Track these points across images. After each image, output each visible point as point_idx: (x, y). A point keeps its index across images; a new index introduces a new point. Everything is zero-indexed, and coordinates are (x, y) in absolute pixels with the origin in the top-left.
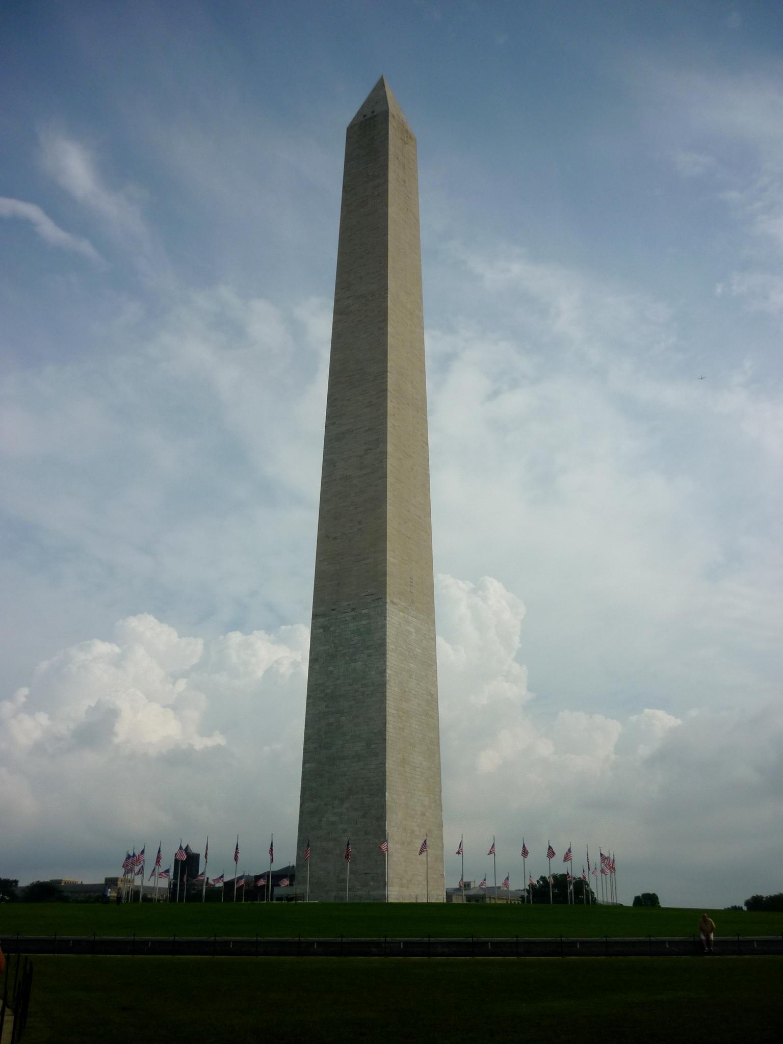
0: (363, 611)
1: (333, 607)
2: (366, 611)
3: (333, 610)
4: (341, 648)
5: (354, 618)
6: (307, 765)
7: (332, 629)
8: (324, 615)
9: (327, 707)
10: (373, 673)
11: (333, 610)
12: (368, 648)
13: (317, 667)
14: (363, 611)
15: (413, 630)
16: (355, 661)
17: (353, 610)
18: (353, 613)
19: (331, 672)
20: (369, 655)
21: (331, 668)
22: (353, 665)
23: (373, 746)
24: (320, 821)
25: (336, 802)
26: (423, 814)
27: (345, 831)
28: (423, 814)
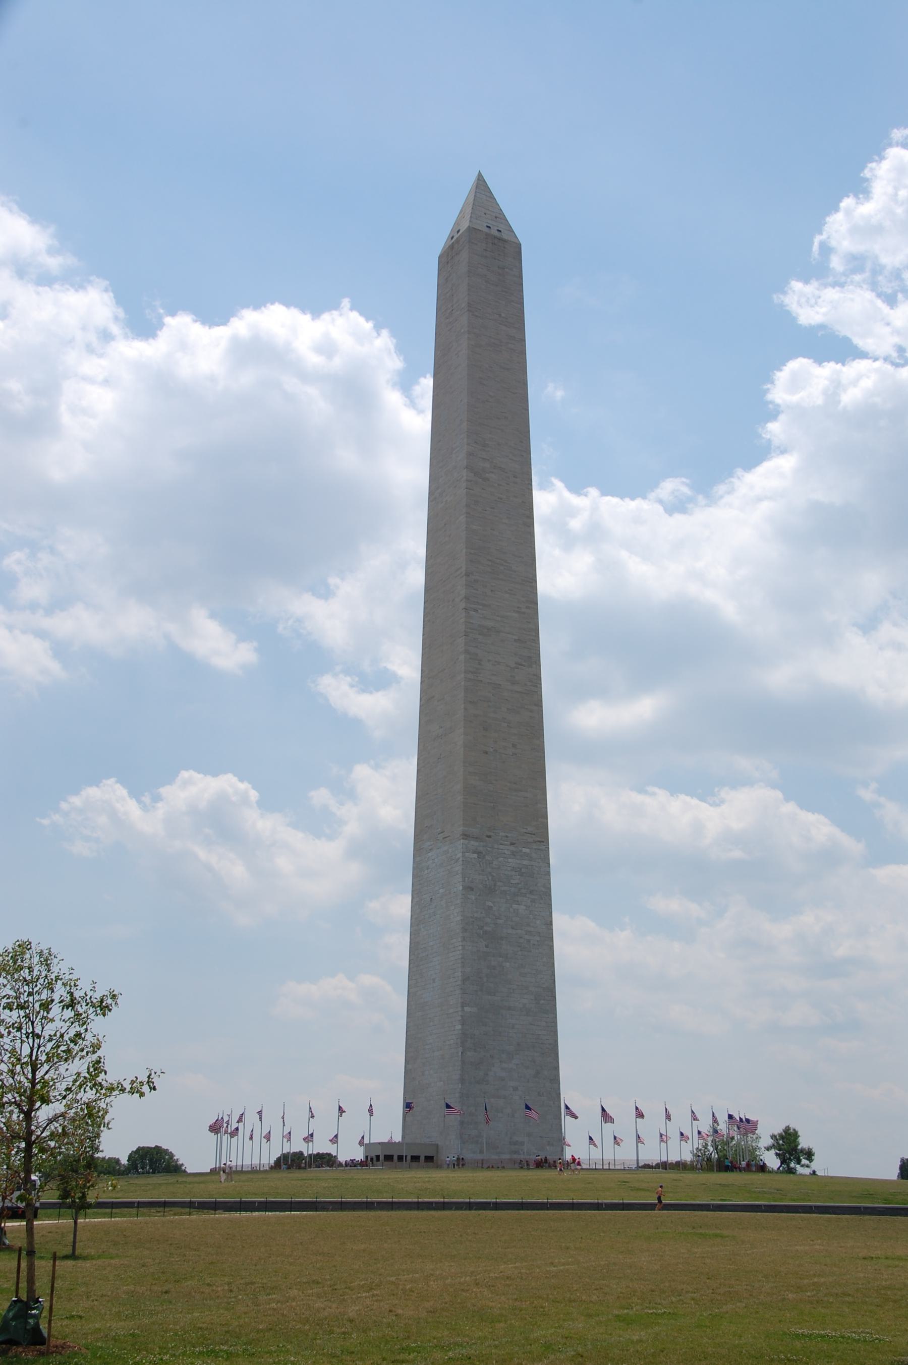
1: (489, 834)
2: (528, 851)
3: (489, 837)
4: (499, 884)
5: (513, 854)
6: (466, 1009)
7: (488, 858)
8: (476, 839)
9: (487, 946)
10: (538, 922)
11: (489, 837)
12: (531, 892)
13: (473, 898)
17: (512, 844)
18: (512, 848)
20: (533, 901)
22: (515, 906)
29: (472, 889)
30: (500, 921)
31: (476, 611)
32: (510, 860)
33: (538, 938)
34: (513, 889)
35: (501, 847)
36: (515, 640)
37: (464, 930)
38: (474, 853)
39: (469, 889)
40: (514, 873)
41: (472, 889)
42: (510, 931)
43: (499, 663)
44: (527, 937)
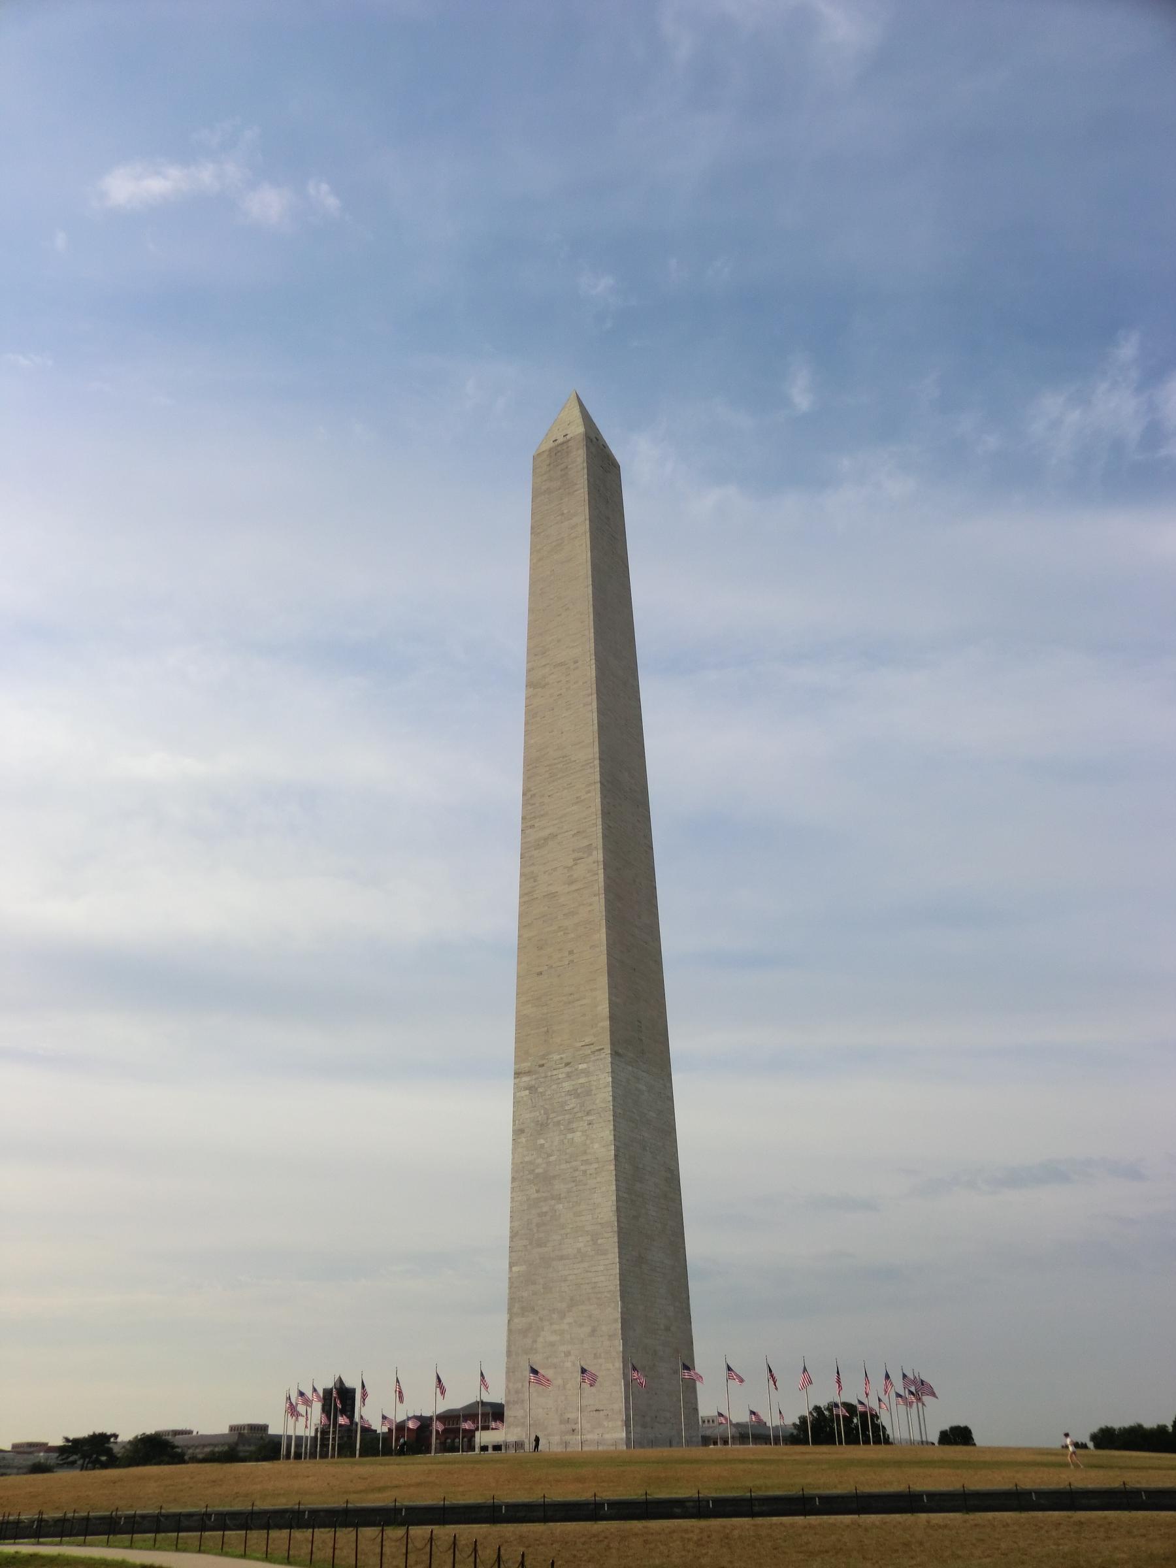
0: (581, 1067)
3: (543, 1065)
5: (569, 1076)
6: (515, 1269)
7: (540, 1090)
8: (529, 1073)
9: (537, 1191)
10: (596, 1146)
11: (543, 1065)
12: (588, 1114)
13: (524, 1140)
14: (581, 1067)
15: (644, 1088)
16: (572, 1131)
17: (567, 1064)
18: (568, 1069)
19: (542, 1146)
21: (542, 1141)
22: (570, 1136)
23: (599, 1241)
24: (535, 1341)
25: (555, 1316)
26: (667, 1329)
27: (568, 1354)
28: (667, 1329)
29: (522, 1131)
30: (552, 1158)
31: (532, 826)
32: (564, 1084)
33: (596, 1166)
34: (567, 1117)
35: (555, 1072)
36: (574, 835)
37: (514, 1179)
38: (526, 1089)
39: (518, 1132)
40: (568, 1098)
41: (522, 1131)
42: (564, 1166)
43: (555, 869)
44: (583, 1168)
